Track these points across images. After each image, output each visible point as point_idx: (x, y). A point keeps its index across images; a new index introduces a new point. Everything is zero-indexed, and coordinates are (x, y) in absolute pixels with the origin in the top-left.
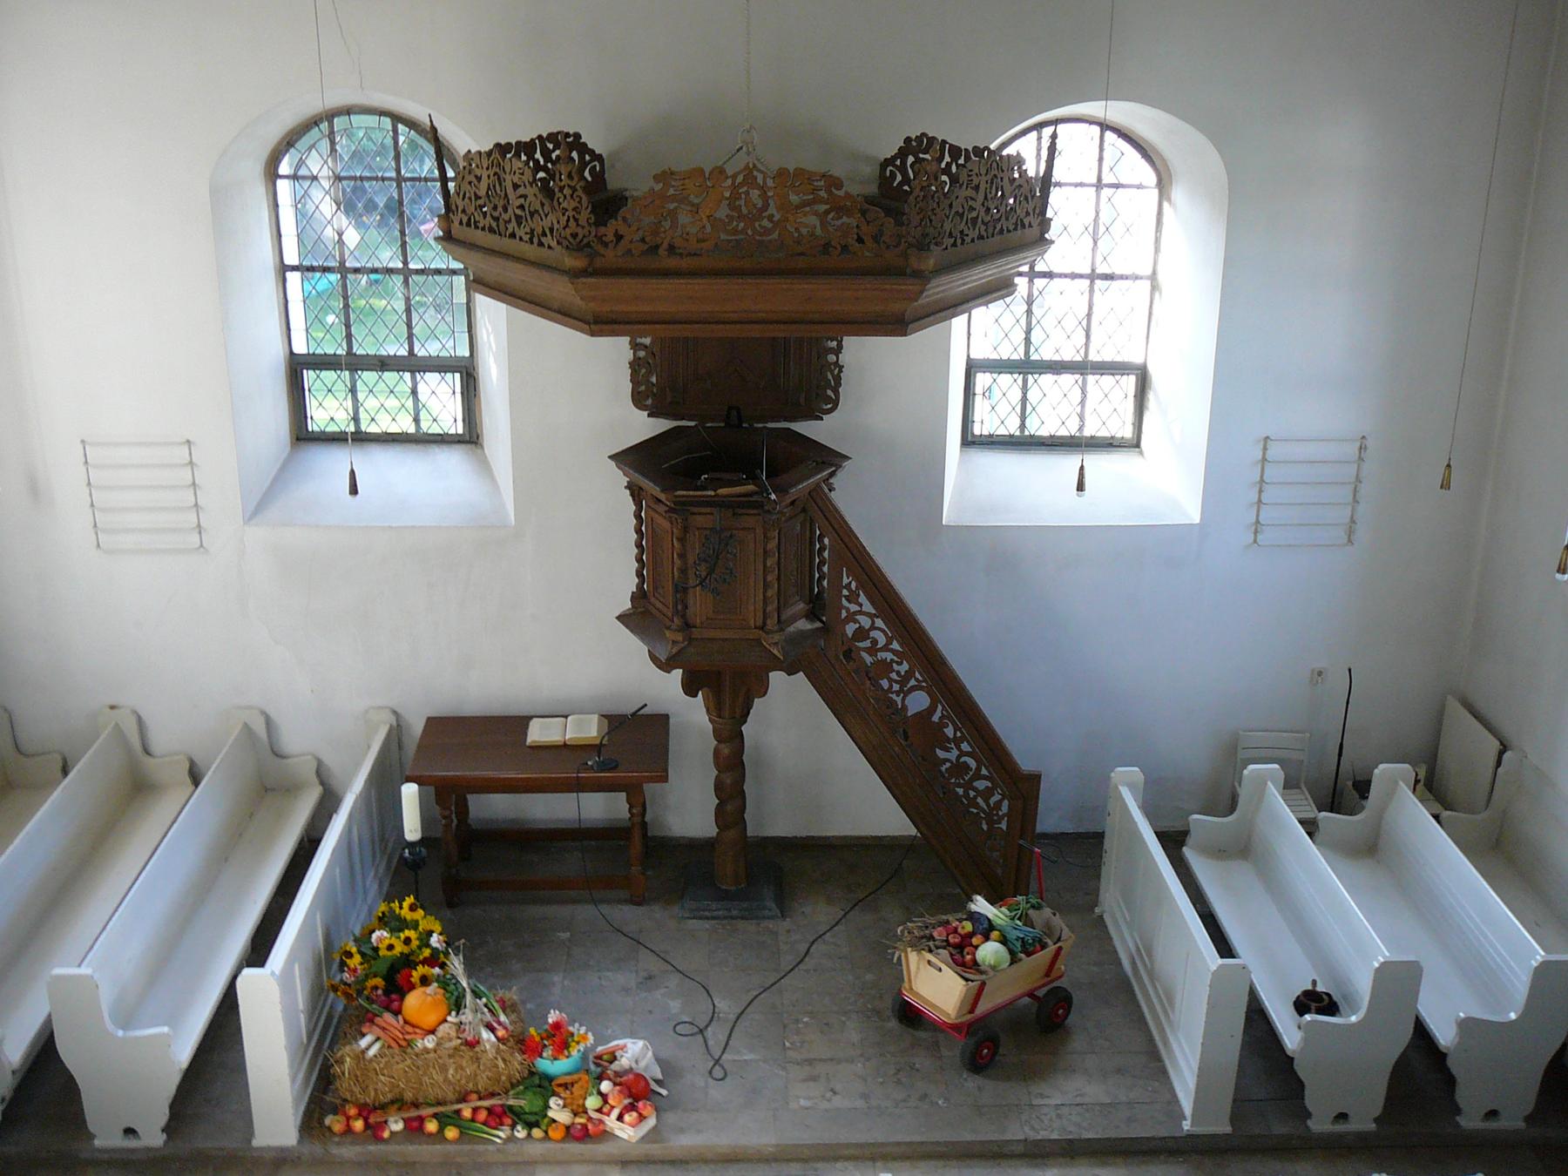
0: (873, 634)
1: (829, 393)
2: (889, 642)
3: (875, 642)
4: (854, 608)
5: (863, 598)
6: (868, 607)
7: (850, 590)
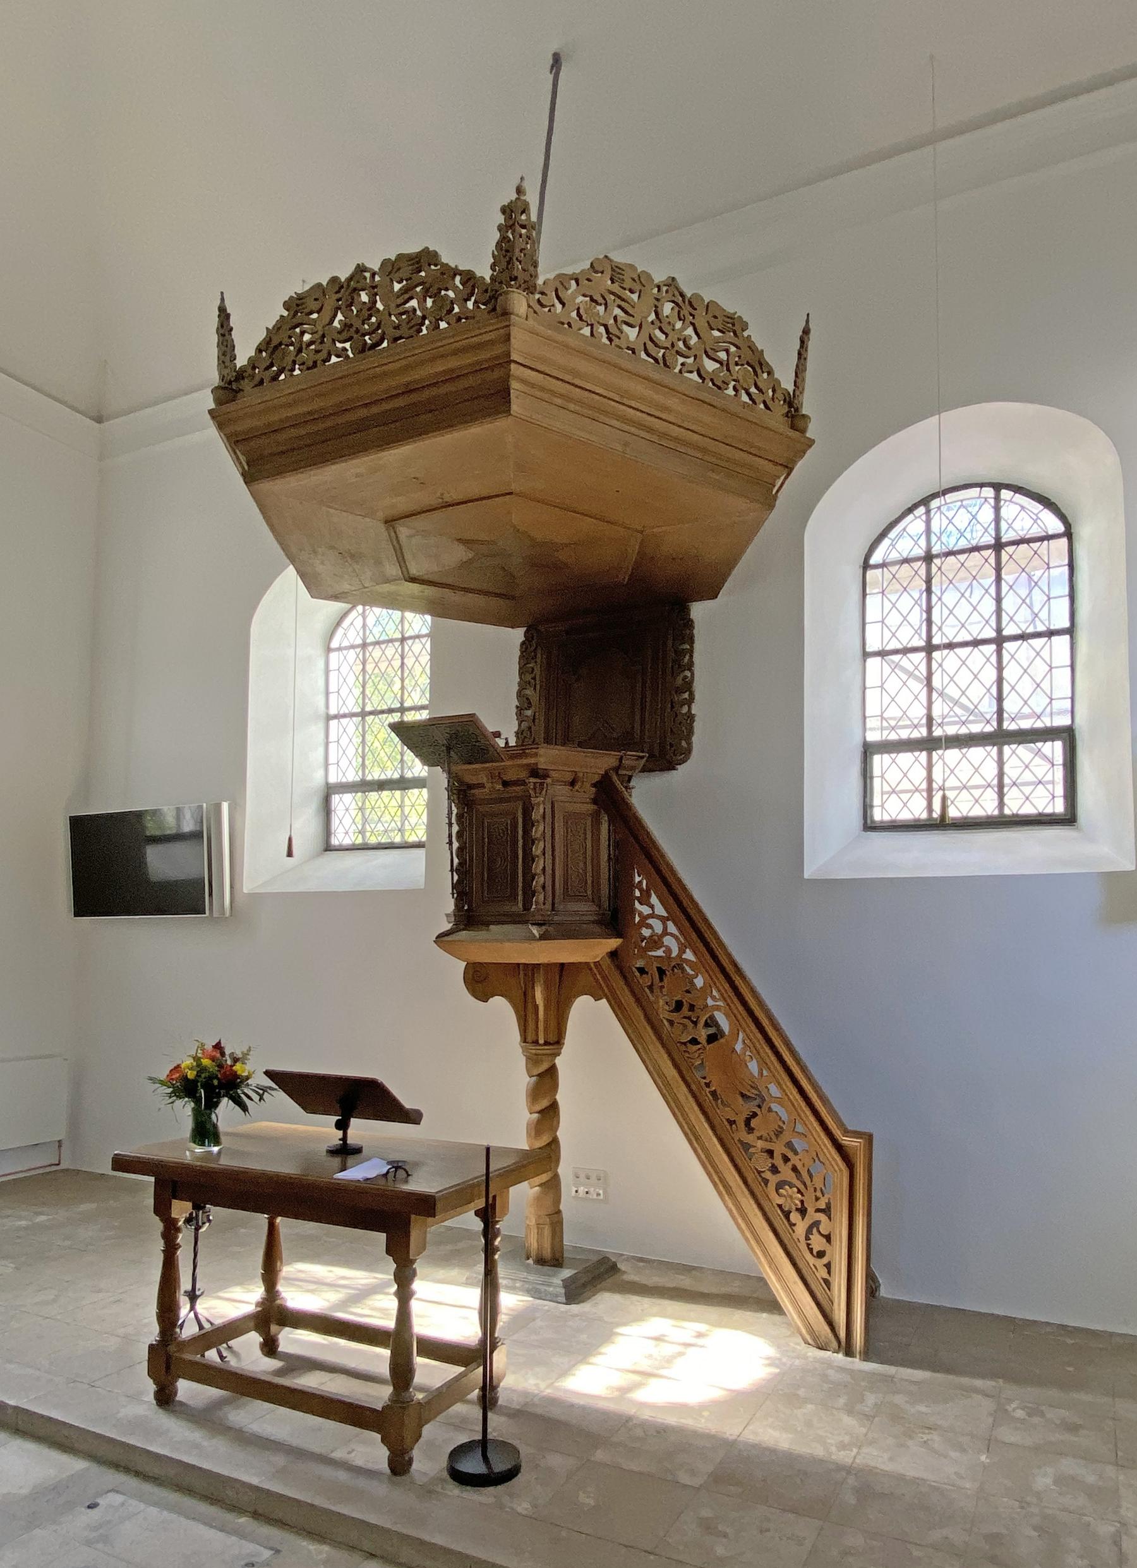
0: (668, 941)
1: (684, 743)
2: (682, 951)
3: (669, 950)
4: (645, 910)
5: (654, 899)
6: (660, 910)
7: (641, 890)
